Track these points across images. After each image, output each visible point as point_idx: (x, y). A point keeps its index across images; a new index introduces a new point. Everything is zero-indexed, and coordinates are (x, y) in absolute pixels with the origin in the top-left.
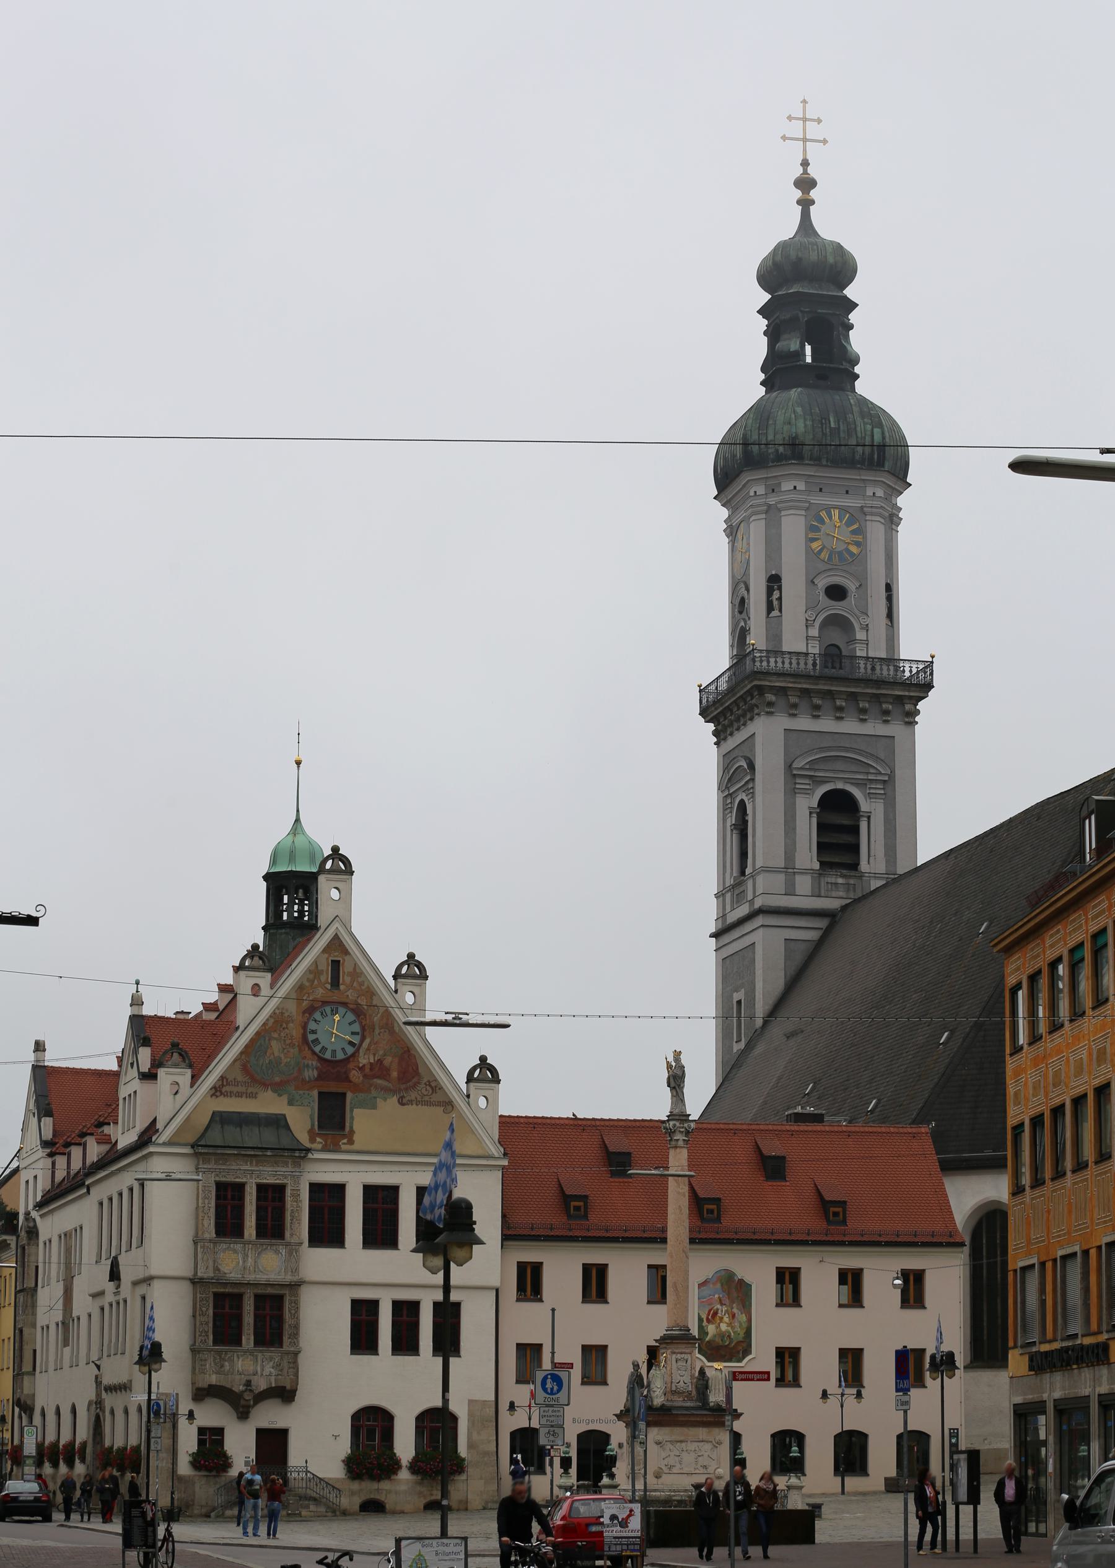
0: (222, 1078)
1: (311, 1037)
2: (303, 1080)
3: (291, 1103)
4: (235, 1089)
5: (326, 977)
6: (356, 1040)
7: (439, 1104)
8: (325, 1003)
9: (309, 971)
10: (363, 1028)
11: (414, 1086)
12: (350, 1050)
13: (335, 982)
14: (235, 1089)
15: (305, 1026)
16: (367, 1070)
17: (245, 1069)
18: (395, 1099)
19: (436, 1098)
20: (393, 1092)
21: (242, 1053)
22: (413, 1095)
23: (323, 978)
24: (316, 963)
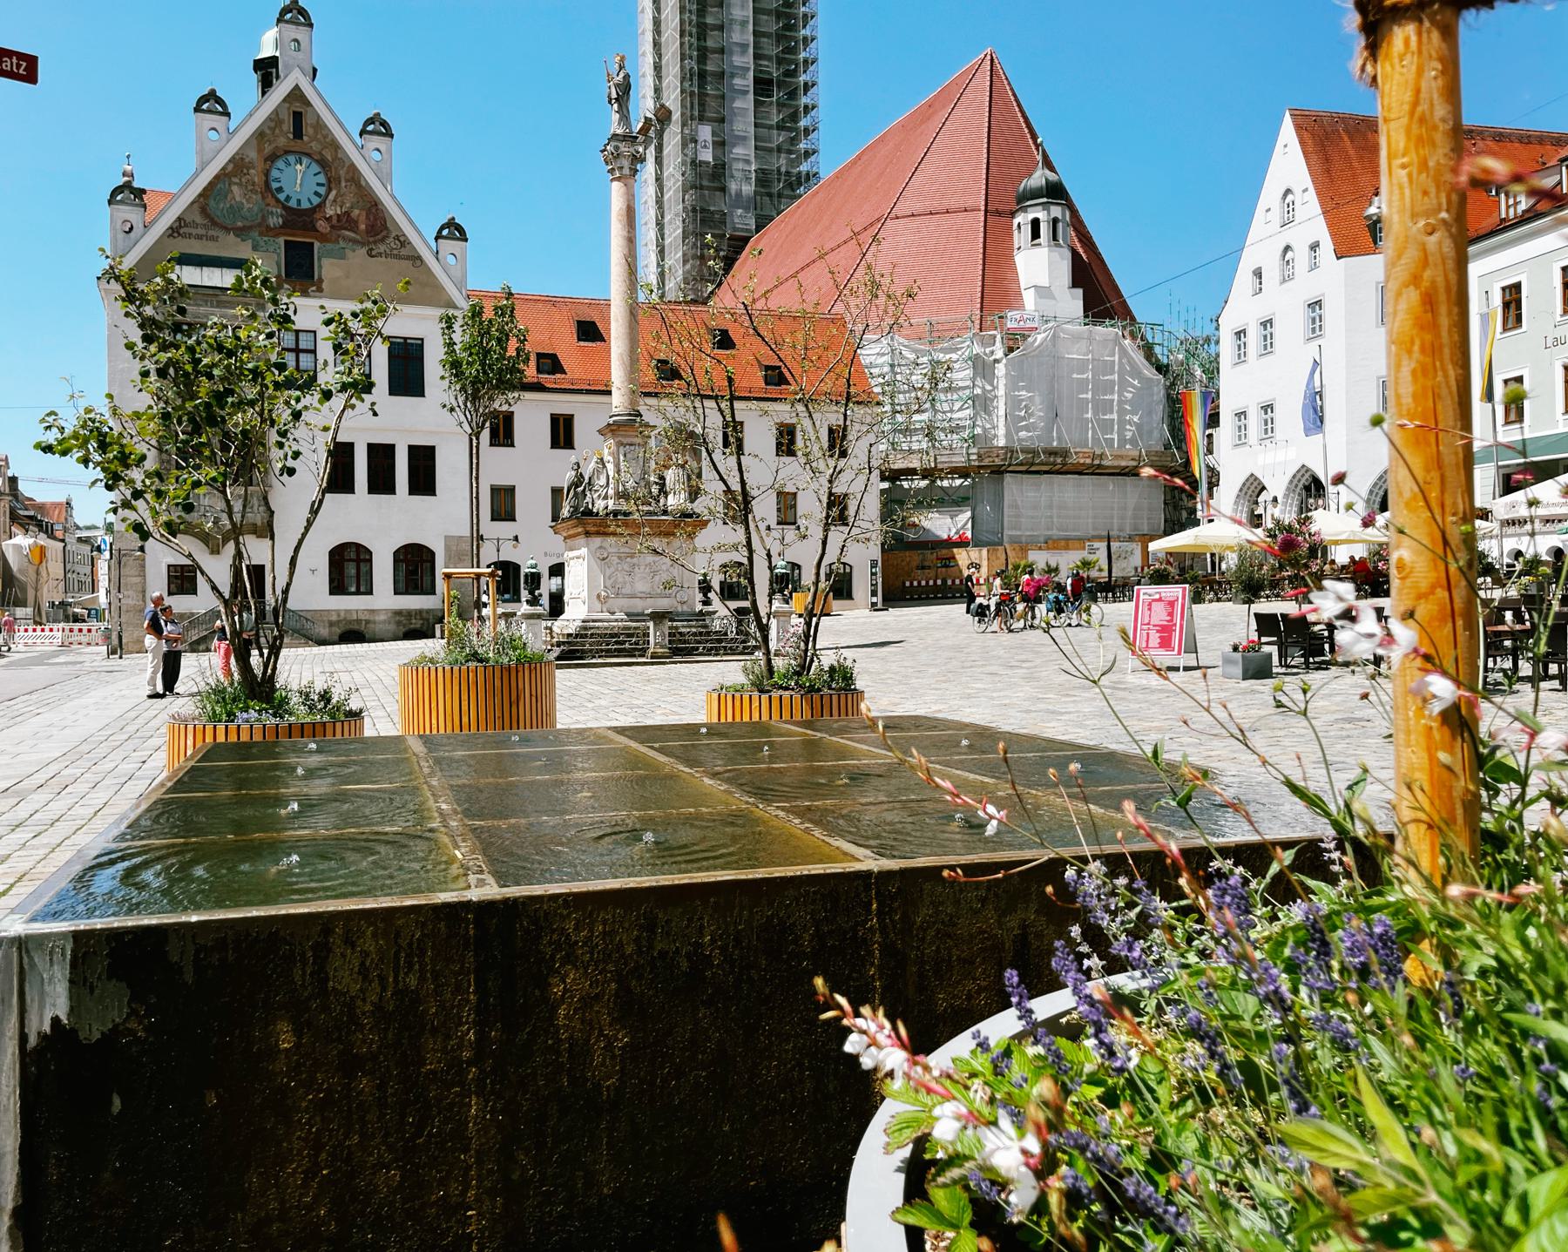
0: (179, 219)
1: (275, 185)
2: (268, 227)
3: (255, 248)
4: (194, 232)
5: (288, 126)
6: (322, 190)
7: (408, 258)
8: (287, 152)
9: (269, 118)
10: (329, 181)
11: (383, 240)
12: (316, 200)
13: (298, 133)
14: (194, 232)
15: (267, 174)
16: (334, 221)
17: (204, 211)
18: (364, 250)
19: (403, 252)
20: (363, 244)
21: (200, 195)
22: (382, 248)
23: (285, 127)
24: (276, 112)
